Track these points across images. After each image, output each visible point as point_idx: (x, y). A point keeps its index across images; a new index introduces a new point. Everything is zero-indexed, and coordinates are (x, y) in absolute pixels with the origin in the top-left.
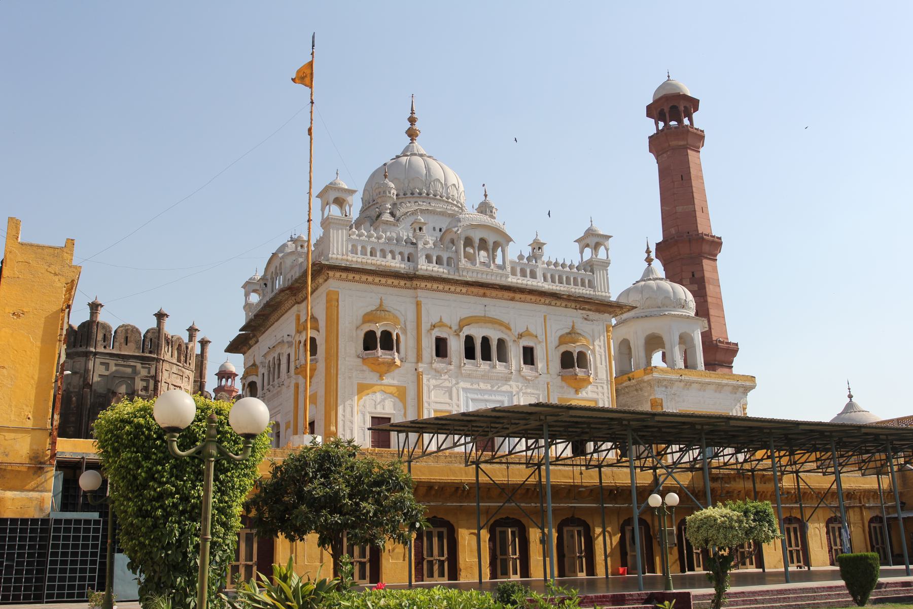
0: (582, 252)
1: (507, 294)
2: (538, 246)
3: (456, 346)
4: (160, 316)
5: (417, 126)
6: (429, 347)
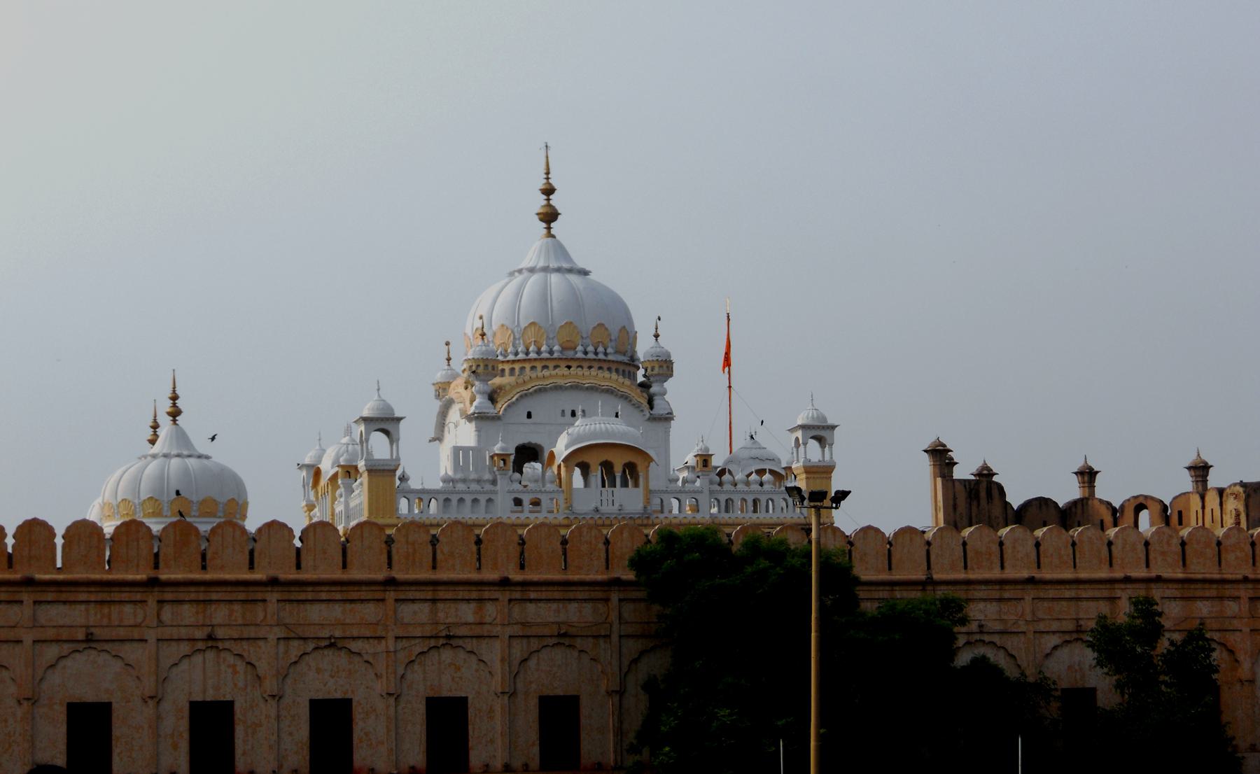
5: (555, 200)
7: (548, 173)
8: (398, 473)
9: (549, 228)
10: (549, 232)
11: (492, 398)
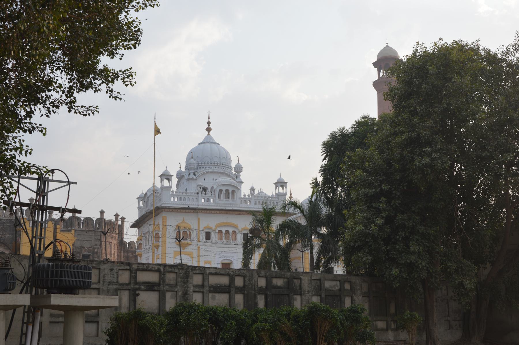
0: (276, 189)
1: (236, 213)
2: (253, 190)
3: (214, 236)
4: (102, 212)
5: (211, 126)
6: (203, 236)
7: (209, 118)
8: (171, 190)
9: (209, 133)
10: (209, 134)
11: (195, 175)
